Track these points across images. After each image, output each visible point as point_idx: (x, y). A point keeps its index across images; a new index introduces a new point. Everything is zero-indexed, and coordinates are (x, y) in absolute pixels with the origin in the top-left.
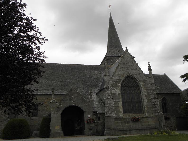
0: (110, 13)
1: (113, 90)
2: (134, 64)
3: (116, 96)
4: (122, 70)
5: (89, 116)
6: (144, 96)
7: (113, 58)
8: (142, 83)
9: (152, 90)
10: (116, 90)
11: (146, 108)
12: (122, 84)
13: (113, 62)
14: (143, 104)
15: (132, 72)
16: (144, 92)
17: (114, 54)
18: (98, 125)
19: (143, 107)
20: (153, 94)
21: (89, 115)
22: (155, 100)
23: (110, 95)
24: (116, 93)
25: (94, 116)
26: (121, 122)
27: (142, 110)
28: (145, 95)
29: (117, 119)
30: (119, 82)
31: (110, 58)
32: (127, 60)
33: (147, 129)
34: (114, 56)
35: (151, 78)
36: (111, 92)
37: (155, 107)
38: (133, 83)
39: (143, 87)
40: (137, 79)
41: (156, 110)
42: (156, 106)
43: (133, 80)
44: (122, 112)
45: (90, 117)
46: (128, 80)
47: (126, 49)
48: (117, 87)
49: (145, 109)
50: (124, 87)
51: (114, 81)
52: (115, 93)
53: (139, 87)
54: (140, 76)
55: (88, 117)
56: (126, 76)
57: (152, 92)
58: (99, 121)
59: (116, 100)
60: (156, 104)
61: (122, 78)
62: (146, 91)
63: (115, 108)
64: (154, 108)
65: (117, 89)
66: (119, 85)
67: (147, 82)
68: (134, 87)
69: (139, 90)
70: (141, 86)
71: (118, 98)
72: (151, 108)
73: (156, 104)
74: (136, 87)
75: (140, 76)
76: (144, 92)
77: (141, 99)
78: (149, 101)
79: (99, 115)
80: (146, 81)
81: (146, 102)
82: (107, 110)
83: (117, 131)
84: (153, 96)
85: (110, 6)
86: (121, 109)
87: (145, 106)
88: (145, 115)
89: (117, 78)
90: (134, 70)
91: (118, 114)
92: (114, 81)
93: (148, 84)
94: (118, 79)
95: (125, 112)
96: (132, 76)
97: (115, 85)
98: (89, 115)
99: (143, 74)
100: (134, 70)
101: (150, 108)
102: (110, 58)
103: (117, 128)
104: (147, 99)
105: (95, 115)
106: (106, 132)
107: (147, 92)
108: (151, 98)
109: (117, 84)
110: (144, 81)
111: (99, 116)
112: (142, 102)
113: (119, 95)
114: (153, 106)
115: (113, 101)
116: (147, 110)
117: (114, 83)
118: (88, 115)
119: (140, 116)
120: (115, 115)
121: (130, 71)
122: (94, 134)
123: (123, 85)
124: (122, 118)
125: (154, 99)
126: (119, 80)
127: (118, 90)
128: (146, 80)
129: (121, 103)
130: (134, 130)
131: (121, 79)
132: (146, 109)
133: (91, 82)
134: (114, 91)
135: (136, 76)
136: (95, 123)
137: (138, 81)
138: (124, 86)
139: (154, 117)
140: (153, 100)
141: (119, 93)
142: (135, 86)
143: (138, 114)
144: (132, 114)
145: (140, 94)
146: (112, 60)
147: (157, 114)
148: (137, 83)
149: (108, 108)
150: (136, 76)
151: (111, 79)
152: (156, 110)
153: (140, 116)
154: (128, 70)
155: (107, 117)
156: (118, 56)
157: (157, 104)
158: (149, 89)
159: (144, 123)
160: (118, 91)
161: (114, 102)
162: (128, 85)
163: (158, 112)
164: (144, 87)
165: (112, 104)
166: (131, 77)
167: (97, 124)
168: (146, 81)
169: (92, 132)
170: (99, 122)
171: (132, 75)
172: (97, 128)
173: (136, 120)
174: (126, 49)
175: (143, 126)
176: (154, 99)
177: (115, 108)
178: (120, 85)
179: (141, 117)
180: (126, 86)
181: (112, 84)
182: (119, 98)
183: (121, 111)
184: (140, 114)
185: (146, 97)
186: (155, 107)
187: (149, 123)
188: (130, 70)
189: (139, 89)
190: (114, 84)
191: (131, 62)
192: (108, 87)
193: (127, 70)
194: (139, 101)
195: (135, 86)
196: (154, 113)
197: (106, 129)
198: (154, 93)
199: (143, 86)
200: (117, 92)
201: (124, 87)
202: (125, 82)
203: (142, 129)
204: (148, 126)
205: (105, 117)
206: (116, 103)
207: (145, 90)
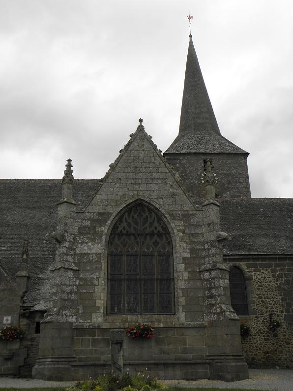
0: (191, 36)
1: (82, 243)
2: (157, 168)
3: (90, 262)
5: (7, 320)
6: (181, 260)
7: (181, 158)
8: (177, 223)
9: (207, 243)
10: (90, 244)
11: (184, 298)
12: (115, 228)
13: (182, 169)
14: (176, 286)
16: (181, 249)
17: (186, 146)
18: (32, 345)
19: (176, 296)
20: (209, 255)
21: (9, 318)
22: (213, 274)
23: (70, 259)
24: (89, 254)
25: (24, 321)
26: (94, 341)
27: (173, 304)
28: (184, 259)
29: (81, 331)
30: (102, 222)
31: (175, 159)
32: (137, 157)
33: (173, 365)
34: (184, 154)
35: (208, 206)
37: (212, 296)
38: (151, 224)
39: (181, 234)
40: (163, 211)
41: (213, 305)
42: (214, 291)
43: (153, 213)
44: (102, 310)
45: (9, 322)
46: (136, 216)
47: (141, 124)
48: (94, 236)
49: (180, 300)
50: (120, 234)
52: (85, 254)
53: (169, 234)
54: (174, 203)
55: (5, 322)
56: (128, 203)
57: (209, 249)
58: (35, 335)
59: (88, 275)
60: (213, 288)
61: (114, 211)
62: (189, 247)
64: (208, 297)
65: (93, 240)
66: (102, 231)
67: (195, 220)
68: (152, 234)
69: (170, 243)
70: (175, 231)
71: (94, 267)
72: (200, 298)
73: (213, 288)
74: (160, 235)
75: (174, 203)
76: (181, 250)
77: (172, 271)
78: (195, 276)
79: (39, 318)
80: (191, 217)
81: (185, 280)
82: (51, 303)
83: (73, 366)
84: (209, 261)
85: (192, 17)
86: (98, 301)
87: (180, 292)
88: (178, 319)
89: (98, 209)
90: (156, 184)
91: (87, 315)
93: (198, 226)
94: (100, 214)
95: (112, 309)
96: (150, 204)
97: (88, 231)
98: (9, 318)
99: (185, 196)
100: (156, 184)
101: (199, 297)
102: (172, 158)
103: (78, 357)
104: (189, 272)
105: (23, 316)
106: (36, 368)
107: (192, 251)
108: (203, 267)
109: (95, 228)
110: (186, 217)
111: (37, 320)
112: (173, 279)
113: (99, 258)
114: (206, 293)
116: (184, 304)
117: (88, 223)
118: (5, 318)
119: (158, 321)
120: (77, 319)
121: (143, 187)
122: (11, 372)
123: (120, 229)
124: (99, 328)
125: (209, 270)
126: (102, 217)
128: (193, 215)
130: (130, 365)
131: (111, 214)
132: (182, 300)
134: (85, 248)
135: (161, 203)
136: (21, 339)
137: (167, 216)
138: (121, 231)
139: (205, 327)
140: (206, 275)
141: (100, 254)
142: (156, 232)
143: (156, 317)
144: (134, 317)
145: (167, 257)
146: (178, 165)
147: (214, 317)
148: (164, 223)
149: (54, 298)
150: (161, 203)
152: (213, 305)
153: (158, 321)
154: (137, 186)
155: (46, 323)
156: (195, 153)
157: (216, 288)
158: (200, 239)
159: (168, 344)
160: (96, 248)
161: (81, 279)
162: (134, 228)
163: (218, 310)
164: (183, 233)
166: (148, 207)
167: (30, 343)
168: (191, 217)
169: (9, 365)
170: (36, 338)
171: (148, 200)
172: (28, 355)
173: (142, 335)
174: (141, 124)
175: (164, 353)
176: (209, 270)
178: (105, 229)
179: (162, 325)
180: (128, 234)
181: (79, 228)
182: (98, 269)
183: (99, 307)
184: (162, 317)
185: (186, 264)
186: (212, 296)
187: (185, 344)
188: (142, 185)
189: (169, 240)
190: (85, 227)
191: (149, 163)
192: (63, 236)
193: (134, 184)
194: (165, 277)
195: (159, 231)
196: (207, 314)
197: (39, 359)
198: (213, 251)
199: (179, 231)
200: (93, 251)
201: (120, 234)
202: (126, 222)
203: (156, 364)
204: (184, 355)
205: (42, 323)
206: (88, 283)
207: (187, 243)
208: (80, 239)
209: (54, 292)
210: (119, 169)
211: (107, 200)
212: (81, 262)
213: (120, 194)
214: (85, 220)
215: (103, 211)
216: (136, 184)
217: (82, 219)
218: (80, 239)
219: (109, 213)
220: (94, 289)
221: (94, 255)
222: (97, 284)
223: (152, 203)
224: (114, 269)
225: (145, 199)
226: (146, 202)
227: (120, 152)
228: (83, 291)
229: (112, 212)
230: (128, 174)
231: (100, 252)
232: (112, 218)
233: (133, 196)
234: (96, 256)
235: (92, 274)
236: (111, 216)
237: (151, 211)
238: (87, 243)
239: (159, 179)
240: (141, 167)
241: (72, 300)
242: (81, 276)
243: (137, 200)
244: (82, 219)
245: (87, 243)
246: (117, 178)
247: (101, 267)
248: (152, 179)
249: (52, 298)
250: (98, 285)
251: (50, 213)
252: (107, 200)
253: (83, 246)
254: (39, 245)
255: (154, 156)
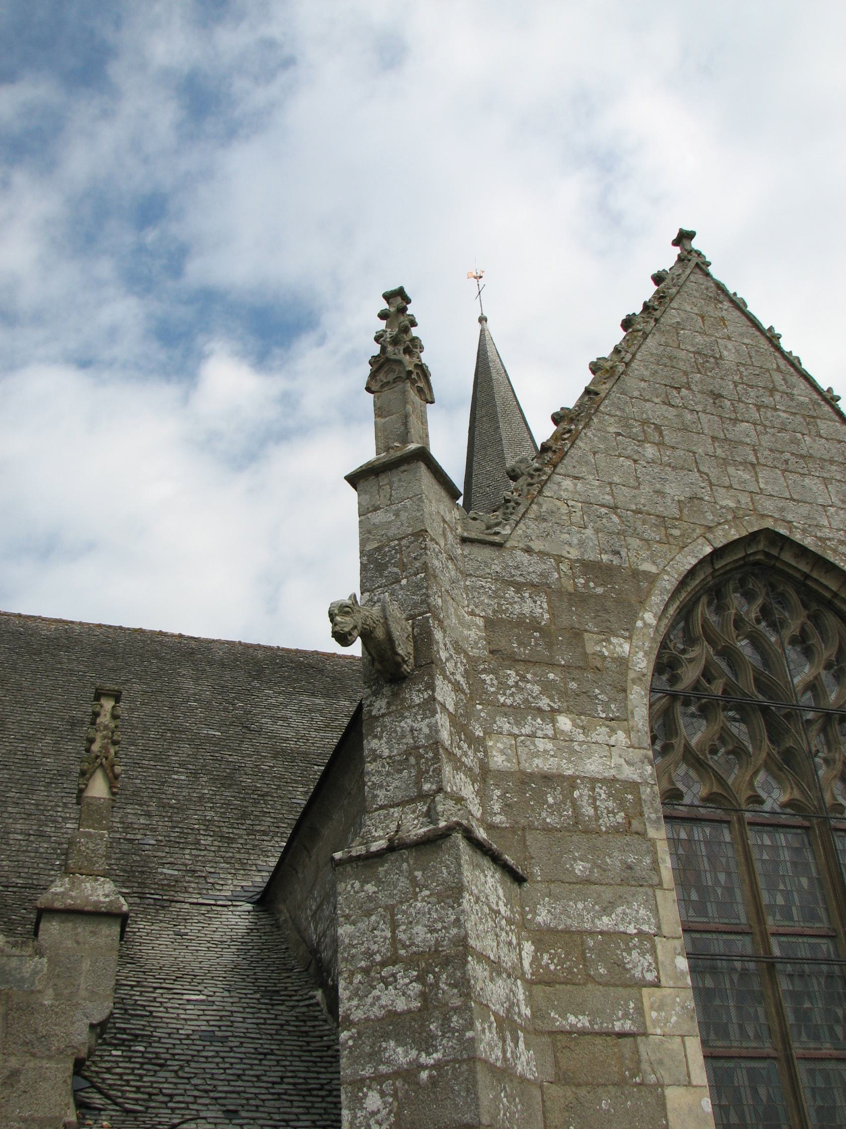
0: (482, 320)
1: (518, 713)
2: (811, 419)
4: (650, 451)
15: (804, 509)
24: (572, 782)
36: (477, 743)
51: (537, 587)
52: (548, 779)
63: (562, 1078)
66: (623, 663)
71: (614, 861)
82: (373, 1101)
86: (674, 1096)
92: (537, 587)
100: (826, 481)
109: (577, 635)
113: (636, 811)
115: (524, 926)
123: (690, 675)
127: (601, 734)
129: (682, 963)
131: (652, 579)
133: (227, 781)
138: (696, 687)
141: (633, 787)
151: (486, 553)
165: (496, 967)
171: (808, 542)
177: (562, 1078)
181: (490, 624)
188: (763, 473)
191: (772, 391)
200: (593, 766)
208: (503, 686)
209: (392, 1014)
210: (643, 384)
211: (614, 508)
212: (531, 827)
213: (675, 491)
214: (519, 587)
215: (605, 557)
216: (735, 464)
217: (497, 578)
218: (503, 686)
219: (636, 574)
220: (640, 1010)
221: (602, 792)
222: (650, 977)
223: (831, 557)
224: (694, 896)
225: (797, 537)
226: (802, 551)
227: (627, 324)
228: (572, 1019)
229: (653, 569)
230: (688, 417)
231: (629, 773)
232: (657, 599)
233: (737, 518)
234: (609, 795)
235: (607, 910)
236: (649, 593)
237: (814, 606)
238: (551, 715)
239: (832, 462)
240: (740, 400)
241: (523, 1079)
242: (539, 919)
243: (753, 537)
244: (497, 578)
245: (551, 715)
246: (644, 423)
247: (655, 867)
248: (802, 457)
249: (375, 1056)
250: (657, 984)
251: (73, 725)
252: (614, 508)
253: (527, 730)
254: (41, 835)
255: (778, 369)
